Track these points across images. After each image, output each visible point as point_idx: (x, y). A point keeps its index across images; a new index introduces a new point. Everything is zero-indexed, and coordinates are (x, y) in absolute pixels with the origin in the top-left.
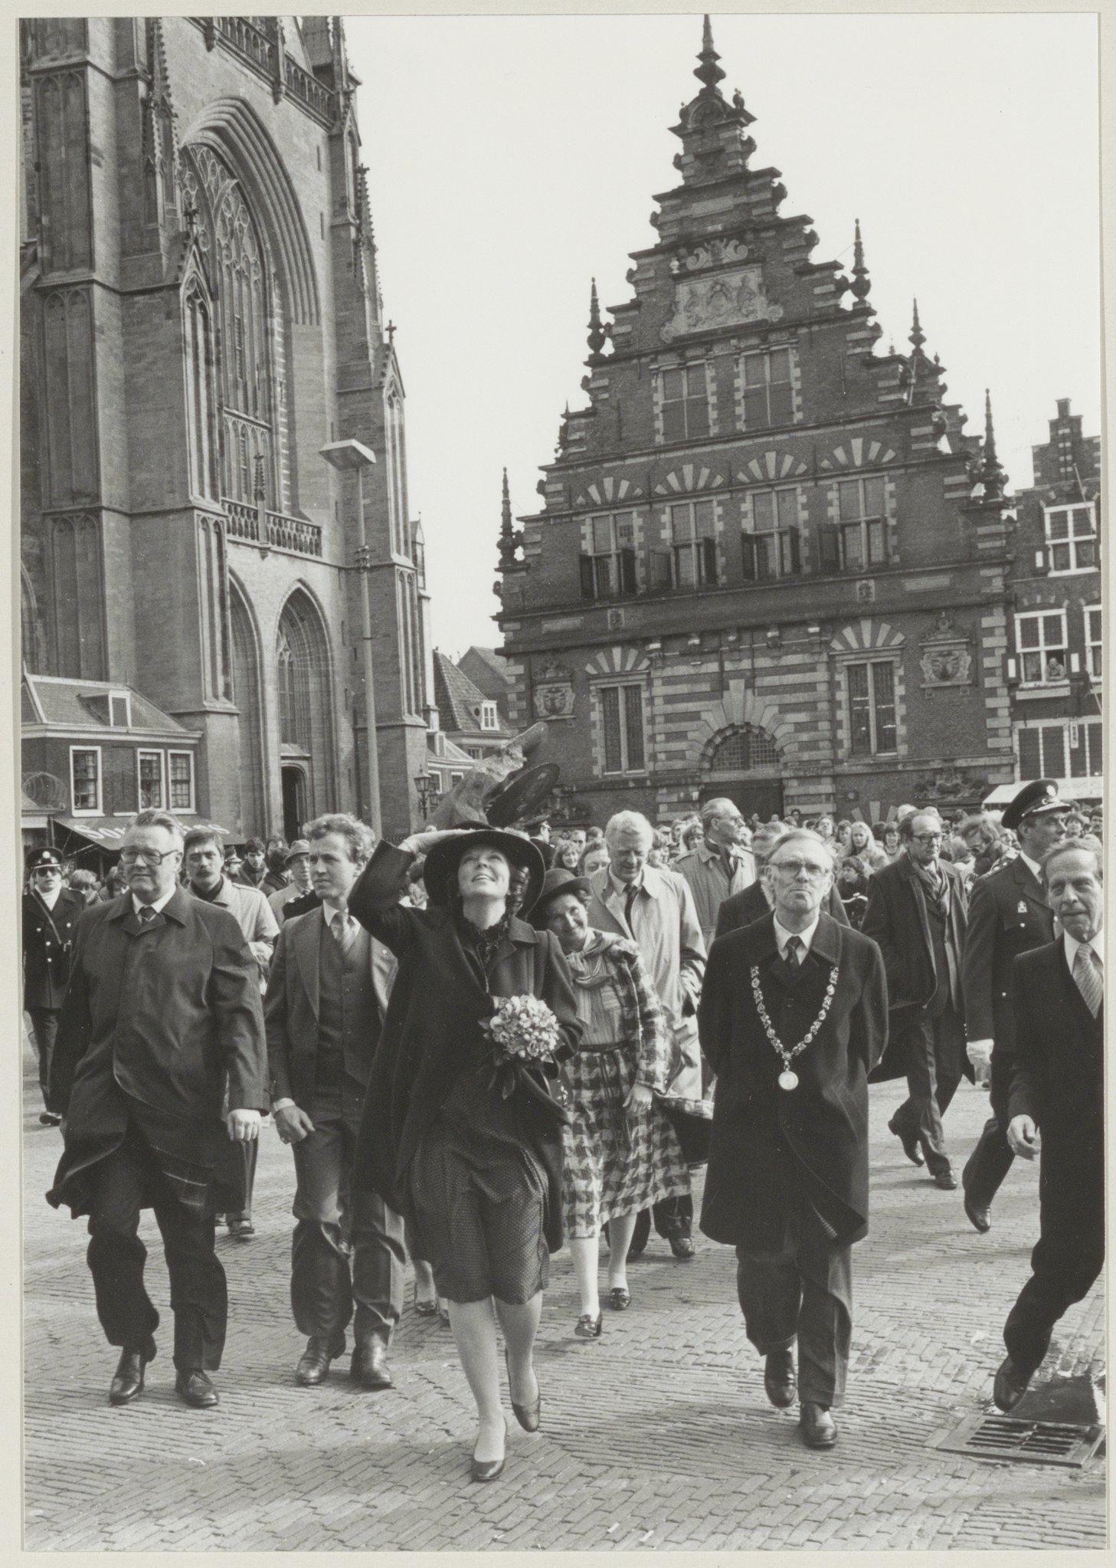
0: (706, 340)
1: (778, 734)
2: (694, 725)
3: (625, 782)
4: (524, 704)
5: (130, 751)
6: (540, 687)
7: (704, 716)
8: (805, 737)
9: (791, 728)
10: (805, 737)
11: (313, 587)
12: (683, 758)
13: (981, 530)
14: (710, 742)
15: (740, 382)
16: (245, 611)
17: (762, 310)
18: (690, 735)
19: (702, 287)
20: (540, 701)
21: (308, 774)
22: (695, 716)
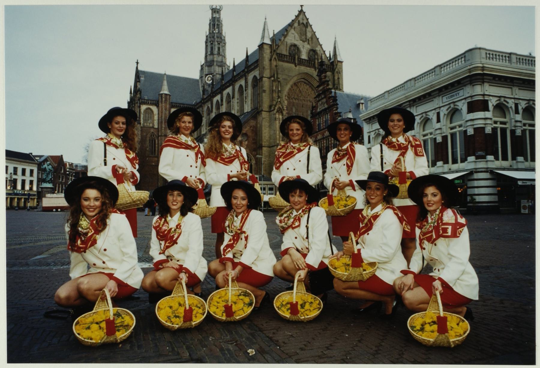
0: (321, 112)
15: (324, 119)
17: (326, 106)
19: (320, 103)
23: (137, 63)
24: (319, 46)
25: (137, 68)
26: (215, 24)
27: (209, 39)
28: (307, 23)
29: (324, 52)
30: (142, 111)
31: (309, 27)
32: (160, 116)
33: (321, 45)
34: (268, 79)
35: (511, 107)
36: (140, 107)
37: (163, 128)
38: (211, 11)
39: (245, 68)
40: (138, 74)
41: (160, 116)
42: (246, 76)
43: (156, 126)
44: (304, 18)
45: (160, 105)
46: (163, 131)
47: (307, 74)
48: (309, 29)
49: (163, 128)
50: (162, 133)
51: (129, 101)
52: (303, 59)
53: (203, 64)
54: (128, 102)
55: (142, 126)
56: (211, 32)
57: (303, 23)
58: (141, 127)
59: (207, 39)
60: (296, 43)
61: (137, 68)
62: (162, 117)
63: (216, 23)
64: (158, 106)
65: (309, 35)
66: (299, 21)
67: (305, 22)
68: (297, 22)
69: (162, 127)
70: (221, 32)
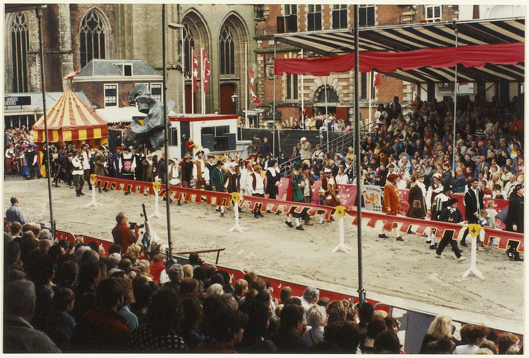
1: (337, 90)
2: (311, 84)
3: (291, 104)
4: (263, 72)
5: (132, 85)
6: (267, 66)
7: (315, 81)
8: (345, 91)
9: (341, 88)
10: (345, 91)
11: (240, 13)
12: (308, 97)
13: (404, 14)
14: (317, 91)
16: (204, 26)
18: (311, 88)
20: (267, 71)
21: (238, 86)
22: (312, 81)
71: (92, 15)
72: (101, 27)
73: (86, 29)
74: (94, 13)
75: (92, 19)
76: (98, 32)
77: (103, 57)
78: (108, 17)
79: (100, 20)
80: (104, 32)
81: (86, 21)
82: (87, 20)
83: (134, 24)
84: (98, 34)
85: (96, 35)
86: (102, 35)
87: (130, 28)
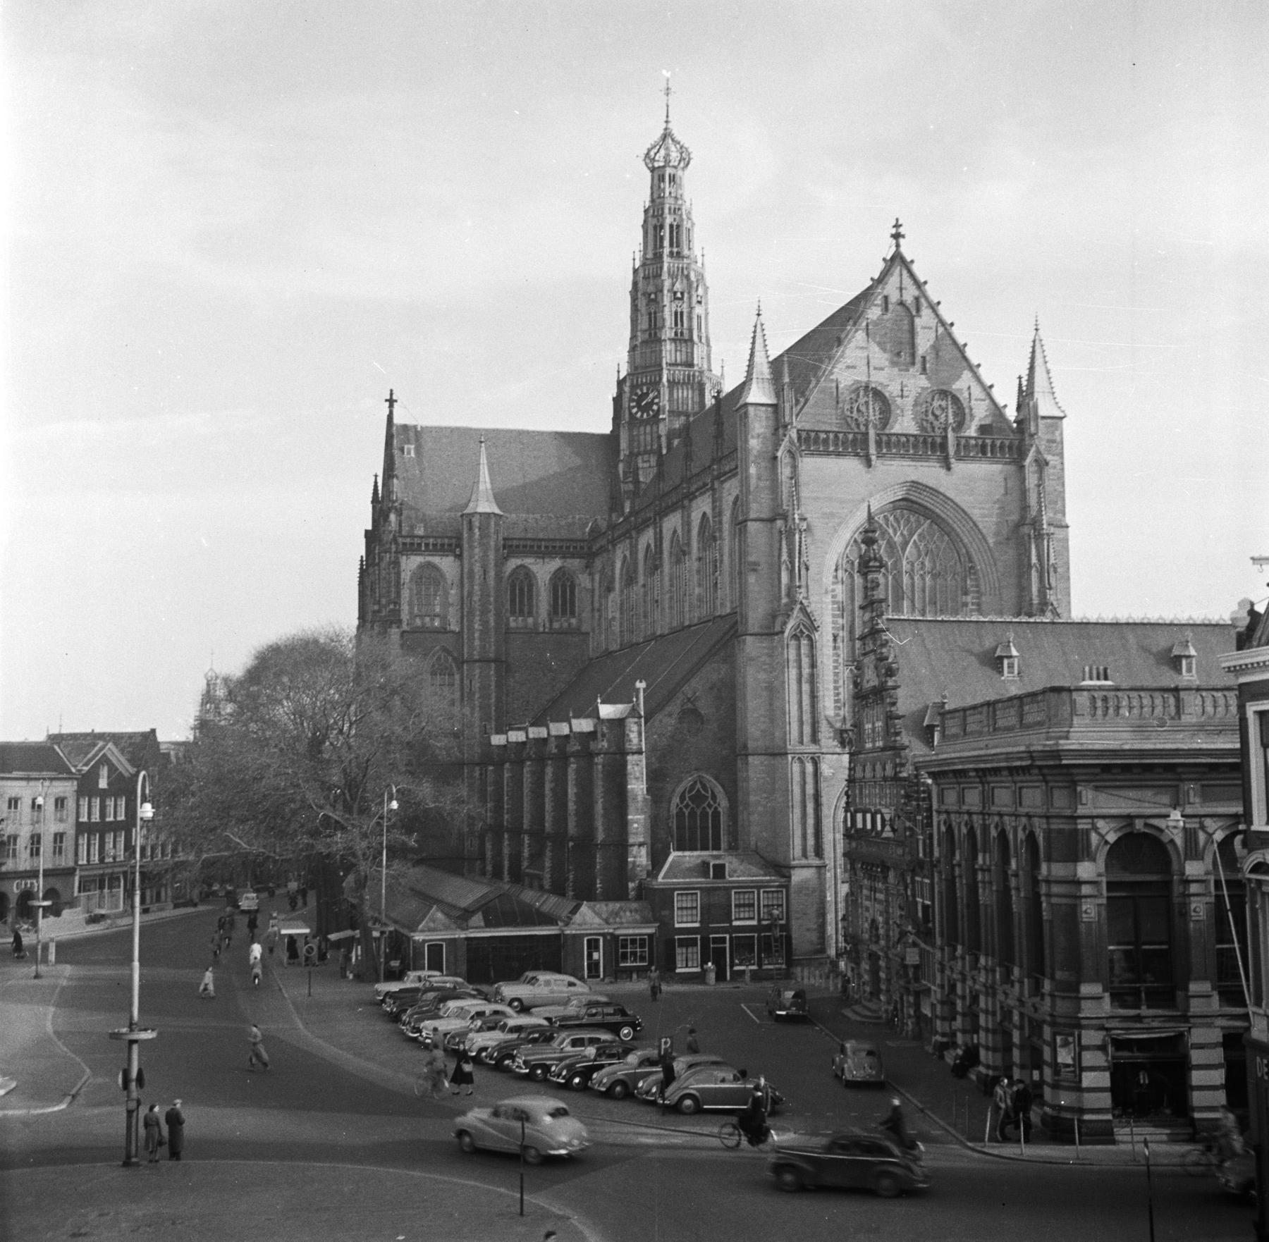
23: (391, 402)
24: (967, 375)
25: (390, 418)
26: (662, 227)
27: (640, 285)
28: (917, 299)
29: (987, 390)
30: (406, 576)
31: (926, 312)
32: (466, 594)
33: (973, 369)
34: (769, 525)
35: (1172, 841)
36: (396, 563)
37: (477, 635)
38: (648, 174)
39: (713, 461)
40: (396, 436)
41: (466, 594)
42: (713, 489)
43: (455, 627)
44: (907, 281)
45: (466, 554)
46: (477, 643)
47: (915, 485)
48: (925, 319)
49: (477, 635)
50: (470, 654)
51: (370, 527)
52: (897, 435)
53: (625, 378)
54: (367, 531)
55: (405, 627)
56: (650, 255)
57: (901, 303)
58: (404, 632)
59: (635, 284)
60: (878, 378)
61: (390, 418)
62: (470, 594)
63: (669, 220)
64: (459, 557)
65: (924, 343)
66: (886, 298)
67: (910, 294)
68: (879, 301)
69: (471, 628)
70: (686, 252)
71: (699, 786)
72: (715, 802)
73: (687, 806)
74: (701, 783)
75: (698, 790)
76: (708, 810)
77: (717, 847)
78: (723, 786)
79: (713, 792)
80: (720, 809)
81: (687, 796)
82: (690, 791)
83: (752, 798)
84: (707, 813)
85: (705, 814)
86: (716, 814)
87: (747, 804)
